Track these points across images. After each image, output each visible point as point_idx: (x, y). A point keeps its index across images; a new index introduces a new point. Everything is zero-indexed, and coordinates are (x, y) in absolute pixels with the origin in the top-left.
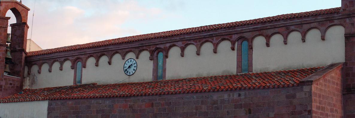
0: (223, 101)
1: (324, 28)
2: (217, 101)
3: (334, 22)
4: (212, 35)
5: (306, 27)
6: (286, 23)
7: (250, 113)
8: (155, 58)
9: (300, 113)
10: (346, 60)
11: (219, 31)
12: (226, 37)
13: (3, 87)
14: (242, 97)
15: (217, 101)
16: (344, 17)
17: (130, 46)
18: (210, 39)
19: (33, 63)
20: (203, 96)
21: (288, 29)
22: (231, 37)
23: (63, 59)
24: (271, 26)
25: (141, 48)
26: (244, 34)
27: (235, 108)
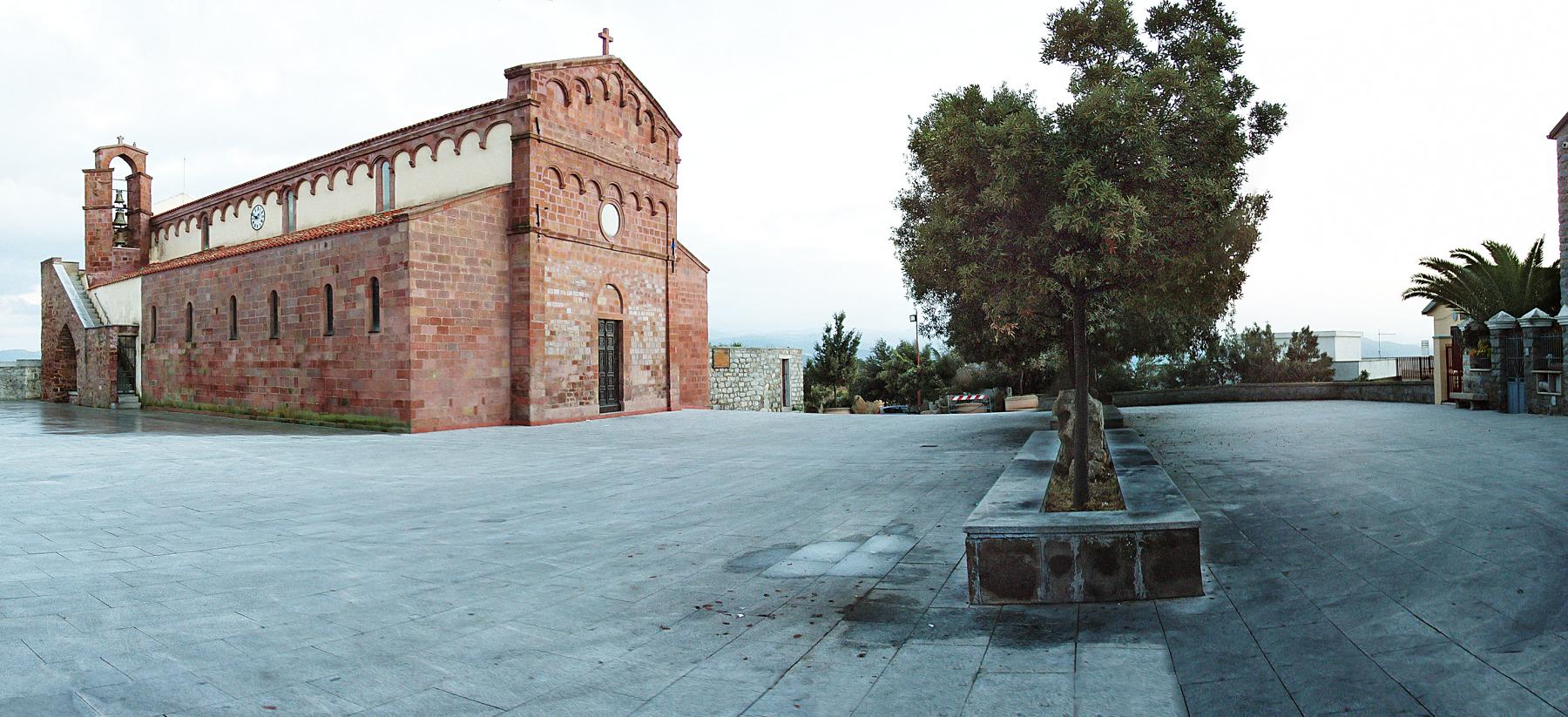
0: (308, 256)
1: (484, 130)
2: (302, 256)
3: (495, 118)
4: (344, 157)
5: (460, 130)
6: (433, 128)
7: (338, 272)
8: (284, 202)
9: (396, 267)
10: (513, 179)
11: (352, 151)
12: (361, 159)
13: (113, 265)
14: (329, 248)
15: (302, 256)
16: (510, 108)
17: (255, 187)
18: (343, 165)
19: (160, 226)
20: (287, 251)
21: (436, 137)
22: (367, 159)
23: (188, 216)
24: (414, 135)
25: (267, 189)
26: (383, 151)
27: (322, 265)
